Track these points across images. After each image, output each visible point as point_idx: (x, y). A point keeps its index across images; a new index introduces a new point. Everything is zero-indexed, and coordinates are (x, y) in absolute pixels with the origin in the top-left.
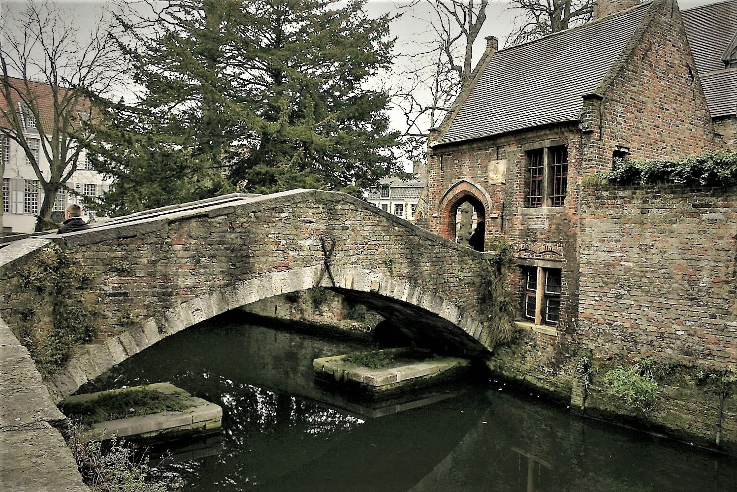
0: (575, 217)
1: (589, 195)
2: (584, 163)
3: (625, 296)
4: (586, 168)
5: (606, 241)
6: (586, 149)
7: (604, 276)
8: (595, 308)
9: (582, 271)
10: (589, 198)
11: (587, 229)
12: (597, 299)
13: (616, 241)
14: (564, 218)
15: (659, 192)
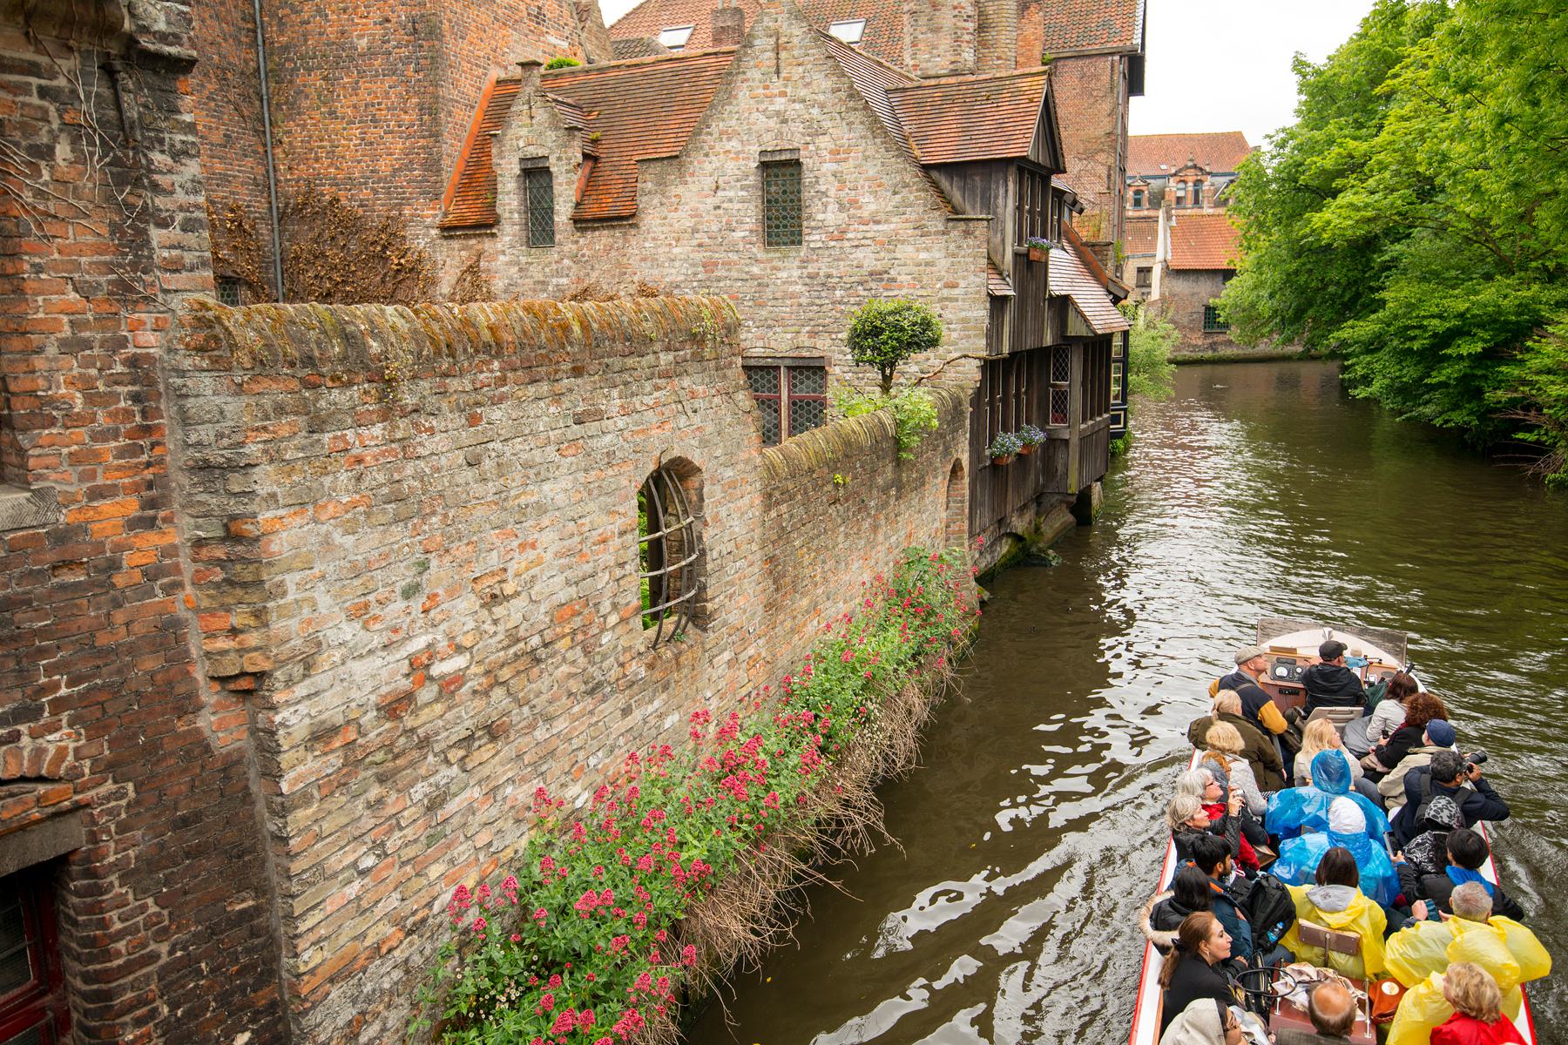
0: (151, 541)
1: (280, 410)
2: (156, 235)
3: (453, 789)
4: (175, 267)
5: (375, 610)
6: (158, 157)
7: (379, 756)
8: (364, 904)
9: (296, 780)
10: (284, 426)
11: (291, 580)
12: (369, 861)
13: (409, 592)
14: (51, 557)
15: (502, 381)
